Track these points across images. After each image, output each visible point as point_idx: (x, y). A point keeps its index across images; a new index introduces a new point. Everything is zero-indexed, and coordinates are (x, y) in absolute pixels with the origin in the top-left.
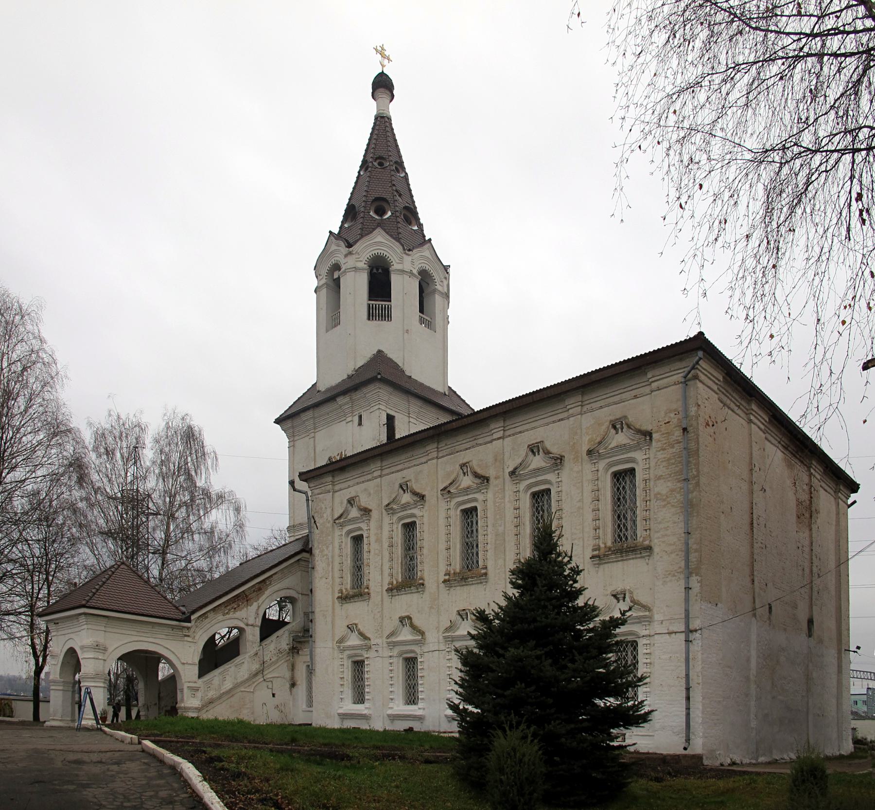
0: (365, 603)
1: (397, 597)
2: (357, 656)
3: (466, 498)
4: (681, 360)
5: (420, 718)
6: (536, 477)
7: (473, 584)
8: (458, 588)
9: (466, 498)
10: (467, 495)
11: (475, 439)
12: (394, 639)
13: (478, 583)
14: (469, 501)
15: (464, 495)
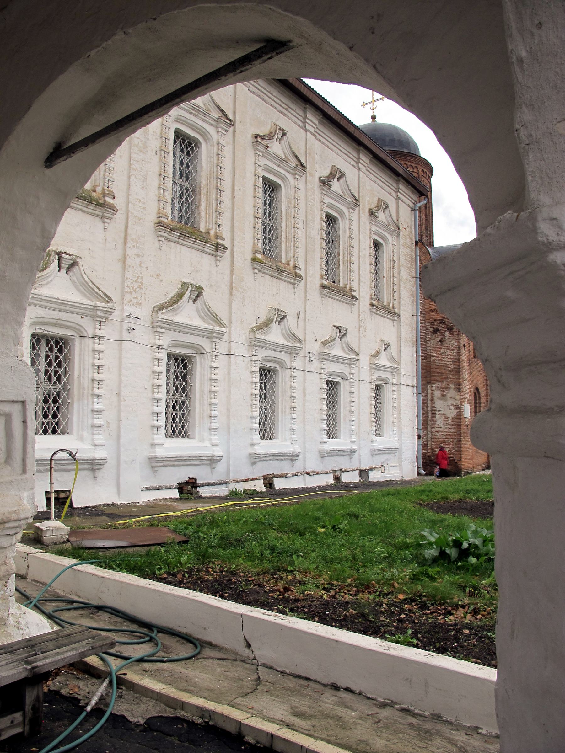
0: (98, 223)
1: (173, 244)
2: (55, 325)
3: (276, 168)
4: (413, 192)
5: (213, 461)
6: (336, 201)
7: (284, 281)
8: (267, 277)
9: (276, 168)
10: (279, 166)
11: (286, 109)
12: (164, 316)
13: (289, 282)
14: (276, 174)
15: (275, 164)
